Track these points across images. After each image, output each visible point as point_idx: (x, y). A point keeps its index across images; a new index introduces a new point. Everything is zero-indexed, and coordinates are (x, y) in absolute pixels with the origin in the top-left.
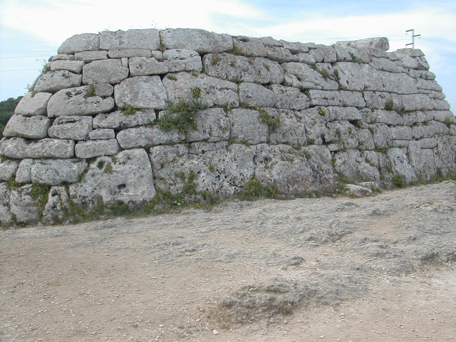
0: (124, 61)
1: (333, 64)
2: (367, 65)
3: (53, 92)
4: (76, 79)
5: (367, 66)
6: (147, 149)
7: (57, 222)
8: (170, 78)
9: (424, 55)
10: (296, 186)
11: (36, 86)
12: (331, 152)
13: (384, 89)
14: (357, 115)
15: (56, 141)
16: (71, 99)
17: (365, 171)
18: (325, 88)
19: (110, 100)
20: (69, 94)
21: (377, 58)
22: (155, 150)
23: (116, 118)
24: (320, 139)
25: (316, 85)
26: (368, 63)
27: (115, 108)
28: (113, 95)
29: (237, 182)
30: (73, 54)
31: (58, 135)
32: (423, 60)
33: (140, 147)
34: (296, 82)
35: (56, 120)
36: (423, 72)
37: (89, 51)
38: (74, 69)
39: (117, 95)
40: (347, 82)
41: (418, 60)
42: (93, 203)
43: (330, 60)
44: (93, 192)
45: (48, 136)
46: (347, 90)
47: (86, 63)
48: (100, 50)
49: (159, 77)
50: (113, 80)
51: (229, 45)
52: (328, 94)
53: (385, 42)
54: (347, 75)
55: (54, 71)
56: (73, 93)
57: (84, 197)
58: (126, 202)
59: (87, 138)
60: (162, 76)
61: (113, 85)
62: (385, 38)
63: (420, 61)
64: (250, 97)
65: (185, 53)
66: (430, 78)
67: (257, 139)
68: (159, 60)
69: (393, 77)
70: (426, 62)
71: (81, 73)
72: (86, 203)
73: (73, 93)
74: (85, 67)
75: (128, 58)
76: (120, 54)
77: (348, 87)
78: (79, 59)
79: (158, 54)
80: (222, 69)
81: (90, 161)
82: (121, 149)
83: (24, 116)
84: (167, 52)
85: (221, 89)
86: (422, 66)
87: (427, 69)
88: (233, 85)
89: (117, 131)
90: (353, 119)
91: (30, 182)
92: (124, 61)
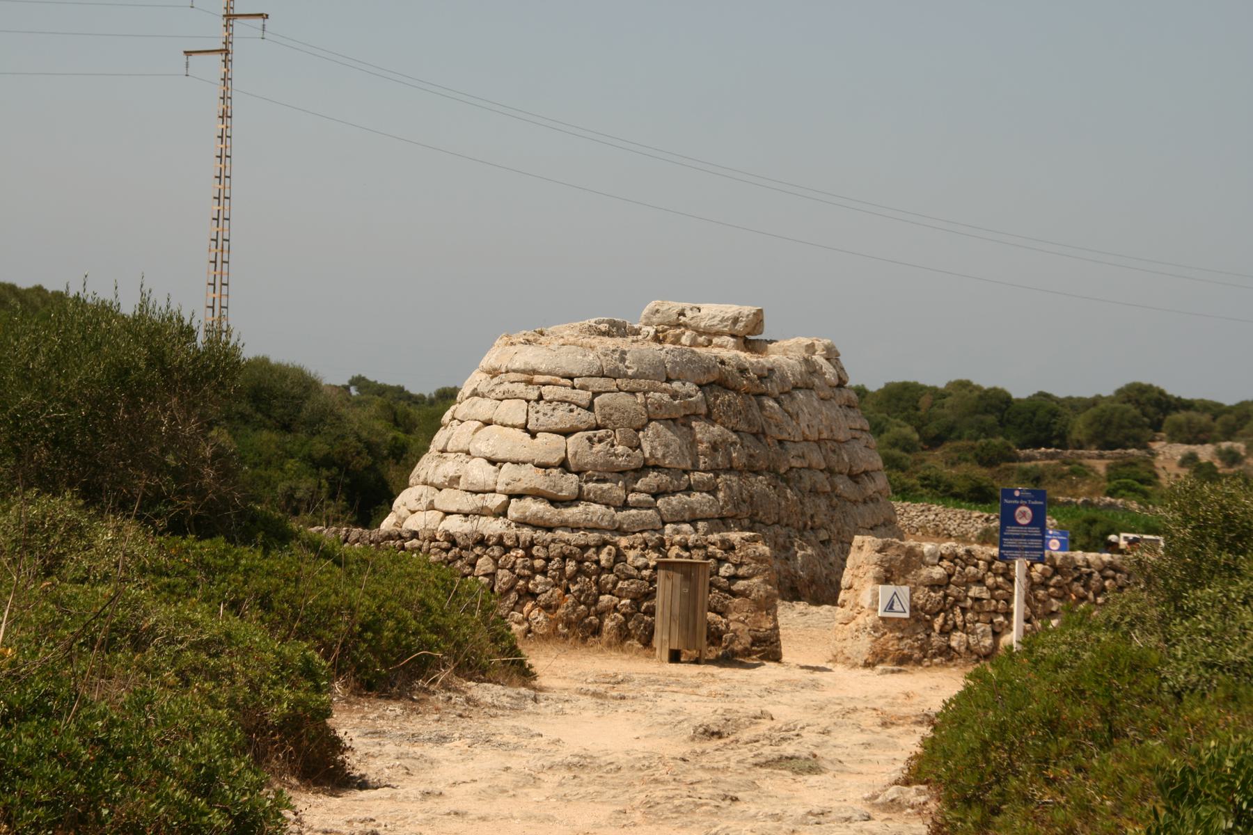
3: (566, 433)
8: (684, 425)
15: (597, 506)
23: (652, 479)
27: (645, 468)
28: (639, 446)
30: (572, 379)
33: (684, 522)
38: (583, 403)
47: (596, 394)
48: (603, 376)
50: (638, 424)
55: (550, 402)
56: (596, 439)
59: (625, 506)
61: (638, 430)
71: (590, 408)
75: (645, 393)
76: (633, 384)
78: (583, 388)
82: (664, 523)
83: (539, 466)
89: (656, 496)
92: (640, 396)
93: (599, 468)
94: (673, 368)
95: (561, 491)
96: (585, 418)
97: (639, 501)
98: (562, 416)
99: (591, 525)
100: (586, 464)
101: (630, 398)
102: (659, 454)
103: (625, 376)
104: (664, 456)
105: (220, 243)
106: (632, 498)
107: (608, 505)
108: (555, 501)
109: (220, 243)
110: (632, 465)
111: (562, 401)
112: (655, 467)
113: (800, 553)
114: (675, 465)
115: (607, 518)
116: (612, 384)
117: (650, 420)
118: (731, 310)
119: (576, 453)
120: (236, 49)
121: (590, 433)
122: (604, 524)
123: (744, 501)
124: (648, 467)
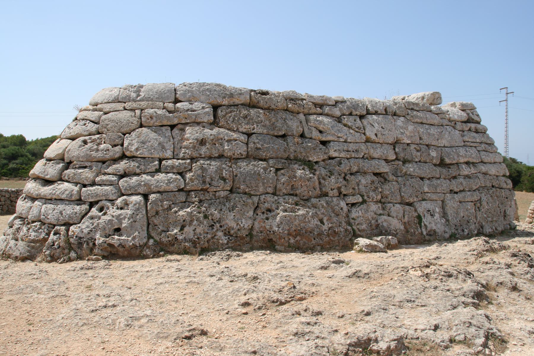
0: (138, 112)
1: (361, 117)
2: (403, 118)
4: (92, 127)
5: (402, 119)
6: (146, 196)
7: (53, 259)
9: (475, 108)
10: (298, 238)
11: (63, 133)
12: (347, 204)
13: (421, 141)
14: (385, 168)
15: (66, 184)
16: (86, 146)
17: (385, 224)
18: (349, 141)
19: (118, 148)
20: (85, 142)
21: (417, 111)
22: (152, 197)
23: (122, 165)
24: (336, 191)
25: (338, 137)
26: (403, 116)
27: (123, 157)
28: (122, 145)
29: (232, 232)
31: (69, 178)
32: (474, 113)
34: (315, 134)
35: (72, 165)
36: (473, 126)
37: (109, 103)
39: (125, 145)
40: (376, 135)
41: (468, 114)
42: (88, 244)
43: (358, 113)
44: (89, 233)
45: (61, 180)
46: (375, 143)
49: (169, 128)
50: (124, 130)
51: (245, 99)
52: (352, 147)
53: (437, 96)
54: (376, 128)
57: (80, 238)
58: (116, 245)
59: (93, 184)
60: (172, 127)
61: (124, 135)
62: (438, 93)
63: (471, 115)
64: (260, 149)
65: (197, 105)
66: (483, 132)
67: (261, 189)
68: (170, 112)
69: (433, 131)
70: (478, 115)
72: (82, 243)
73: (88, 141)
74: (104, 117)
75: (142, 110)
76: (135, 105)
77: (377, 140)
78: (100, 110)
79: (171, 105)
80: (233, 121)
81: (92, 205)
84: (178, 105)
85: (229, 141)
86: (473, 119)
87: (479, 123)
88: (243, 138)
90: (378, 171)
91: (40, 221)
92: (138, 112)
93: (81, 159)
94: (184, 95)
95: (47, 175)
96: (88, 128)
97: (107, 180)
98: (78, 129)
99: (54, 197)
100: (73, 157)
101: (128, 114)
102: (133, 148)
103: (134, 101)
104: (137, 150)
105: (507, 136)
106: (98, 179)
107: (76, 184)
108: (47, 182)
109: (507, 136)
110: (107, 156)
111: (83, 119)
112: (132, 158)
113: (282, 214)
114: (146, 155)
115: (67, 192)
116: (120, 106)
117: (141, 126)
118: (421, 94)
119: (69, 150)
120: (509, 99)
121: (87, 138)
122: (63, 196)
123: (224, 179)
124: (126, 157)
